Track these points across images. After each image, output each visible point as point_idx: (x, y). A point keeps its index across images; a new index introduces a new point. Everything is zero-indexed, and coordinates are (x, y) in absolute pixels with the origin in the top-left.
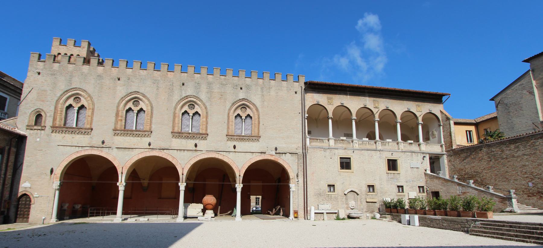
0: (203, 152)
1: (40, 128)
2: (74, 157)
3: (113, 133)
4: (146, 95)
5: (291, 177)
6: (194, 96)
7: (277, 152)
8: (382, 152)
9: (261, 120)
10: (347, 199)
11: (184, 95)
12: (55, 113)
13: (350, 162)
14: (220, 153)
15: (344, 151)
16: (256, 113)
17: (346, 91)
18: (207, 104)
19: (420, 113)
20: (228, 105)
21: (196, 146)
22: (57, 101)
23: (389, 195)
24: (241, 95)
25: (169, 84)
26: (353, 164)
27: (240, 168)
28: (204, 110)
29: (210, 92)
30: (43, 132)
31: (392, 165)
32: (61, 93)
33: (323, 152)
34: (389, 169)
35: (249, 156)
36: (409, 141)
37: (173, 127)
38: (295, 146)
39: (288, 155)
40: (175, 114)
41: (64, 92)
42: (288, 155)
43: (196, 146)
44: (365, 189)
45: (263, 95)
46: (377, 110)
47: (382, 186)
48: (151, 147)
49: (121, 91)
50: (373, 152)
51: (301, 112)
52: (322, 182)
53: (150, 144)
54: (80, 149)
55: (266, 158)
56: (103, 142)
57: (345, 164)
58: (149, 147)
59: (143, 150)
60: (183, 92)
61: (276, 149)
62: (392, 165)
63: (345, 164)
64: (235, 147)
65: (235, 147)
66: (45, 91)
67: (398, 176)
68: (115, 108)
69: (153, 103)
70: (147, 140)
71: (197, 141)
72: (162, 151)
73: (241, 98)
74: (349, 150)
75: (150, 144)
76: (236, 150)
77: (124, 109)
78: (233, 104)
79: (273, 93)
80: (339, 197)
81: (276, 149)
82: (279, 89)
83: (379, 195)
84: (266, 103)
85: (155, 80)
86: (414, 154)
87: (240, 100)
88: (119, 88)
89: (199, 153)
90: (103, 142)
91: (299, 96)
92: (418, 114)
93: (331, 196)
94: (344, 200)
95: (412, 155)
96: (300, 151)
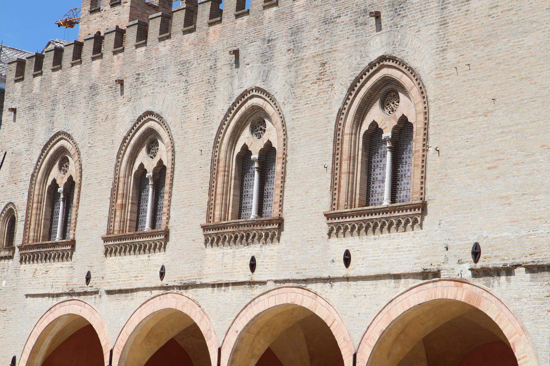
0: (270, 285)
1: (6, 253)
2: (45, 323)
3: (101, 246)
4: (165, 116)
6: (258, 89)
7: (479, 265)
9: (431, 131)
11: (238, 93)
12: (28, 209)
14: (309, 286)
16: (421, 107)
18: (286, 110)
20: (340, 92)
21: (253, 266)
22: (33, 176)
24: (377, 47)
25: (209, 64)
27: (357, 339)
28: (281, 133)
29: (295, 64)
30: (11, 262)
32: (39, 152)
35: (387, 288)
37: (211, 207)
40: (215, 162)
41: (43, 151)
43: (253, 266)
45: (444, 23)
48: (165, 282)
49: (125, 118)
53: (162, 275)
54: (55, 301)
55: (439, 296)
56: (88, 278)
58: (159, 283)
59: (148, 294)
60: (236, 82)
61: (476, 253)
64: (347, 260)
65: (347, 260)
66: (20, 154)
68: (111, 175)
69: (175, 137)
70: (158, 259)
71: (254, 250)
72: (183, 291)
73: (373, 57)
75: (162, 275)
76: (352, 271)
77: (131, 169)
78: (352, 88)
81: (476, 253)
84: (450, 55)
85: (183, 64)
87: (371, 65)
88: (122, 110)
89: (258, 290)
90: (88, 278)
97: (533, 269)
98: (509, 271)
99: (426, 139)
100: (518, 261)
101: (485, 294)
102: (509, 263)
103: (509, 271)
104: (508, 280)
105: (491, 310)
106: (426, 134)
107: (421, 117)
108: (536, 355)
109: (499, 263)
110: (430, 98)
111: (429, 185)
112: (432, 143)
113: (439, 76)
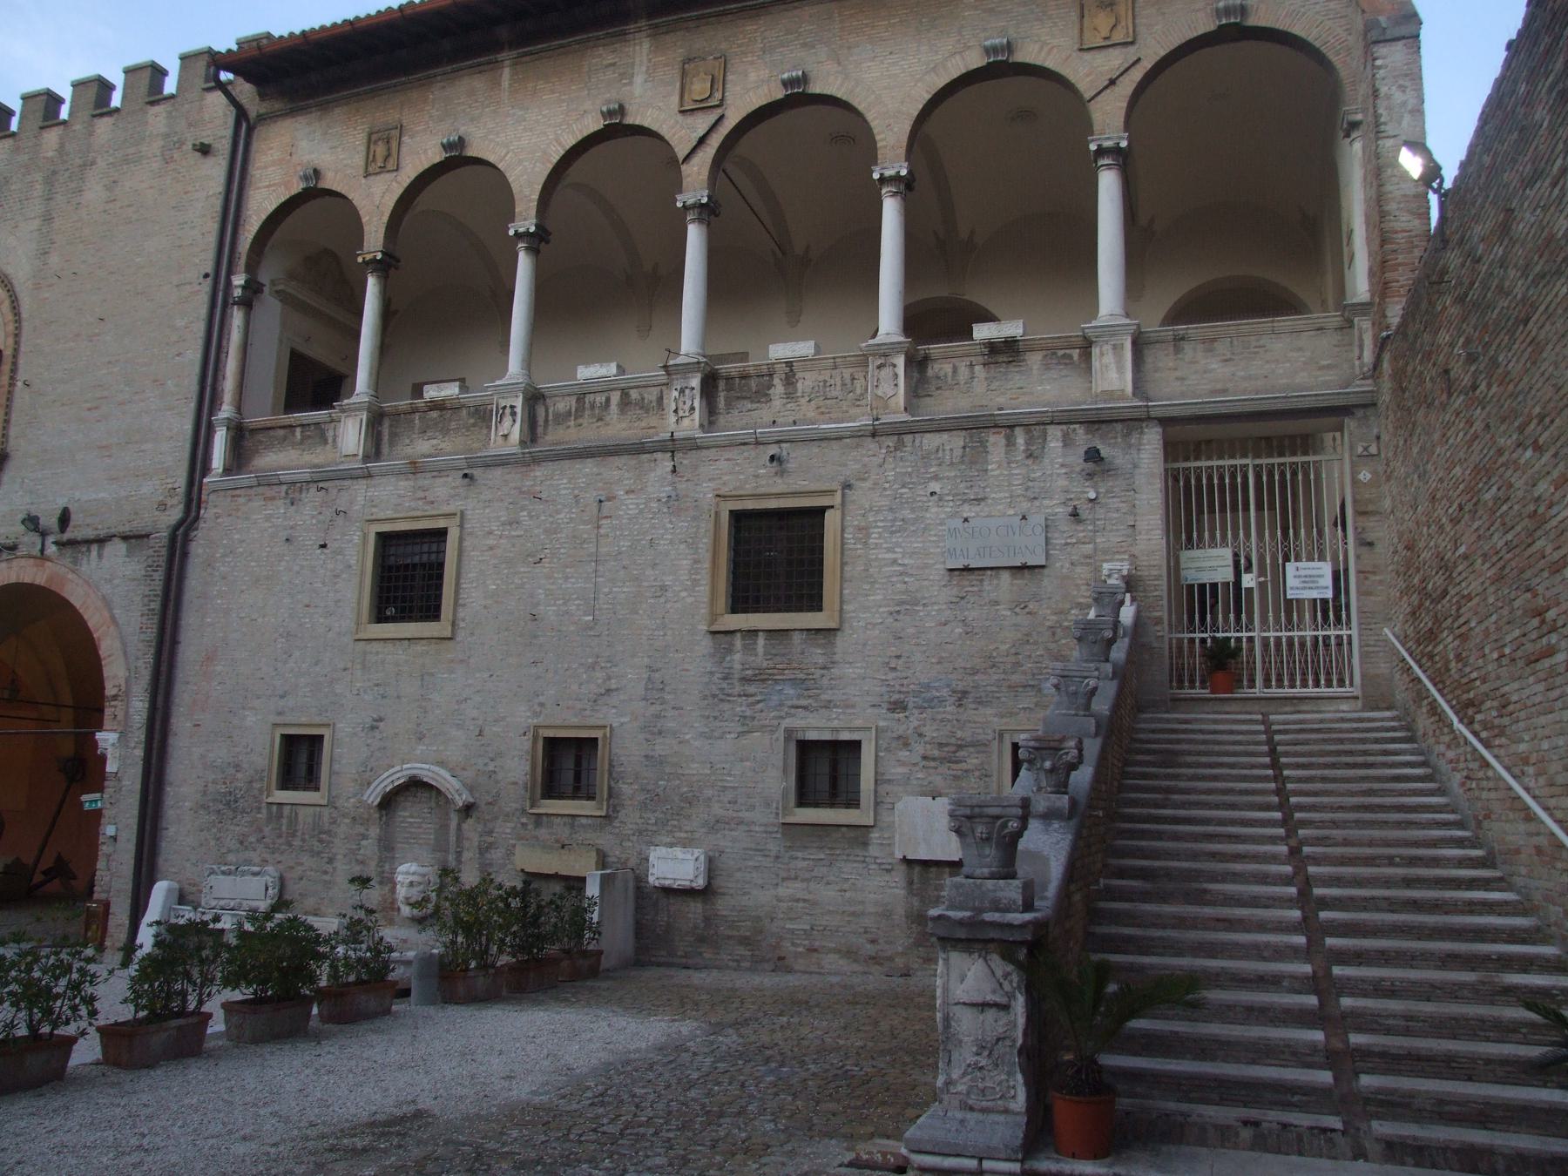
5: (110, 690)
7: (66, 536)
8: (685, 460)
10: (387, 847)
13: (435, 571)
15: (404, 484)
17: (497, 47)
19: (1113, 60)
23: (716, 825)
26: (475, 580)
31: (775, 559)
33: (280, 507)
34: (740, 602)
36: (982, 332)
38: (150, 489)
39: (117, 549)
42: (117, 549)
44: (517, 766)
46: (702, 123)
47: (661, 747)
50: (618, 471)
51: (209, 267)
52: (251, 719)
55: (13, 580)
57: (408, 579)
61: (65, 519)
62: (775, 559)
63: (408, 579)
67: (817, 655)
74: (440, 472)
79: (94, 192)
80: (343, 828)
82: (126, 161)
83: (630, 817)
84: (54, 260)
86: (996, 440)
91: (214, 172)
92: (1084, 72)
93: (293, 821)
94: (369, 847)
95: (975, 456)
96: (176, 514)
97: (125, 538)
98: (101, 541)
99: (14, 371)
100: (113, 531)
101: (70, 576)
102: (102, 533)
103: (101, 541)
104: (100, 556)
105: (76, 595)
106: (15, 364)
107: (11, 341)
108: (125, 653)
109: (90, 533)
110: (24, 315)
111: (13, 432)
112: (22, 376)
113: (37, 287)
